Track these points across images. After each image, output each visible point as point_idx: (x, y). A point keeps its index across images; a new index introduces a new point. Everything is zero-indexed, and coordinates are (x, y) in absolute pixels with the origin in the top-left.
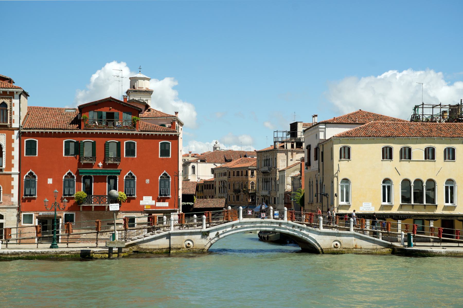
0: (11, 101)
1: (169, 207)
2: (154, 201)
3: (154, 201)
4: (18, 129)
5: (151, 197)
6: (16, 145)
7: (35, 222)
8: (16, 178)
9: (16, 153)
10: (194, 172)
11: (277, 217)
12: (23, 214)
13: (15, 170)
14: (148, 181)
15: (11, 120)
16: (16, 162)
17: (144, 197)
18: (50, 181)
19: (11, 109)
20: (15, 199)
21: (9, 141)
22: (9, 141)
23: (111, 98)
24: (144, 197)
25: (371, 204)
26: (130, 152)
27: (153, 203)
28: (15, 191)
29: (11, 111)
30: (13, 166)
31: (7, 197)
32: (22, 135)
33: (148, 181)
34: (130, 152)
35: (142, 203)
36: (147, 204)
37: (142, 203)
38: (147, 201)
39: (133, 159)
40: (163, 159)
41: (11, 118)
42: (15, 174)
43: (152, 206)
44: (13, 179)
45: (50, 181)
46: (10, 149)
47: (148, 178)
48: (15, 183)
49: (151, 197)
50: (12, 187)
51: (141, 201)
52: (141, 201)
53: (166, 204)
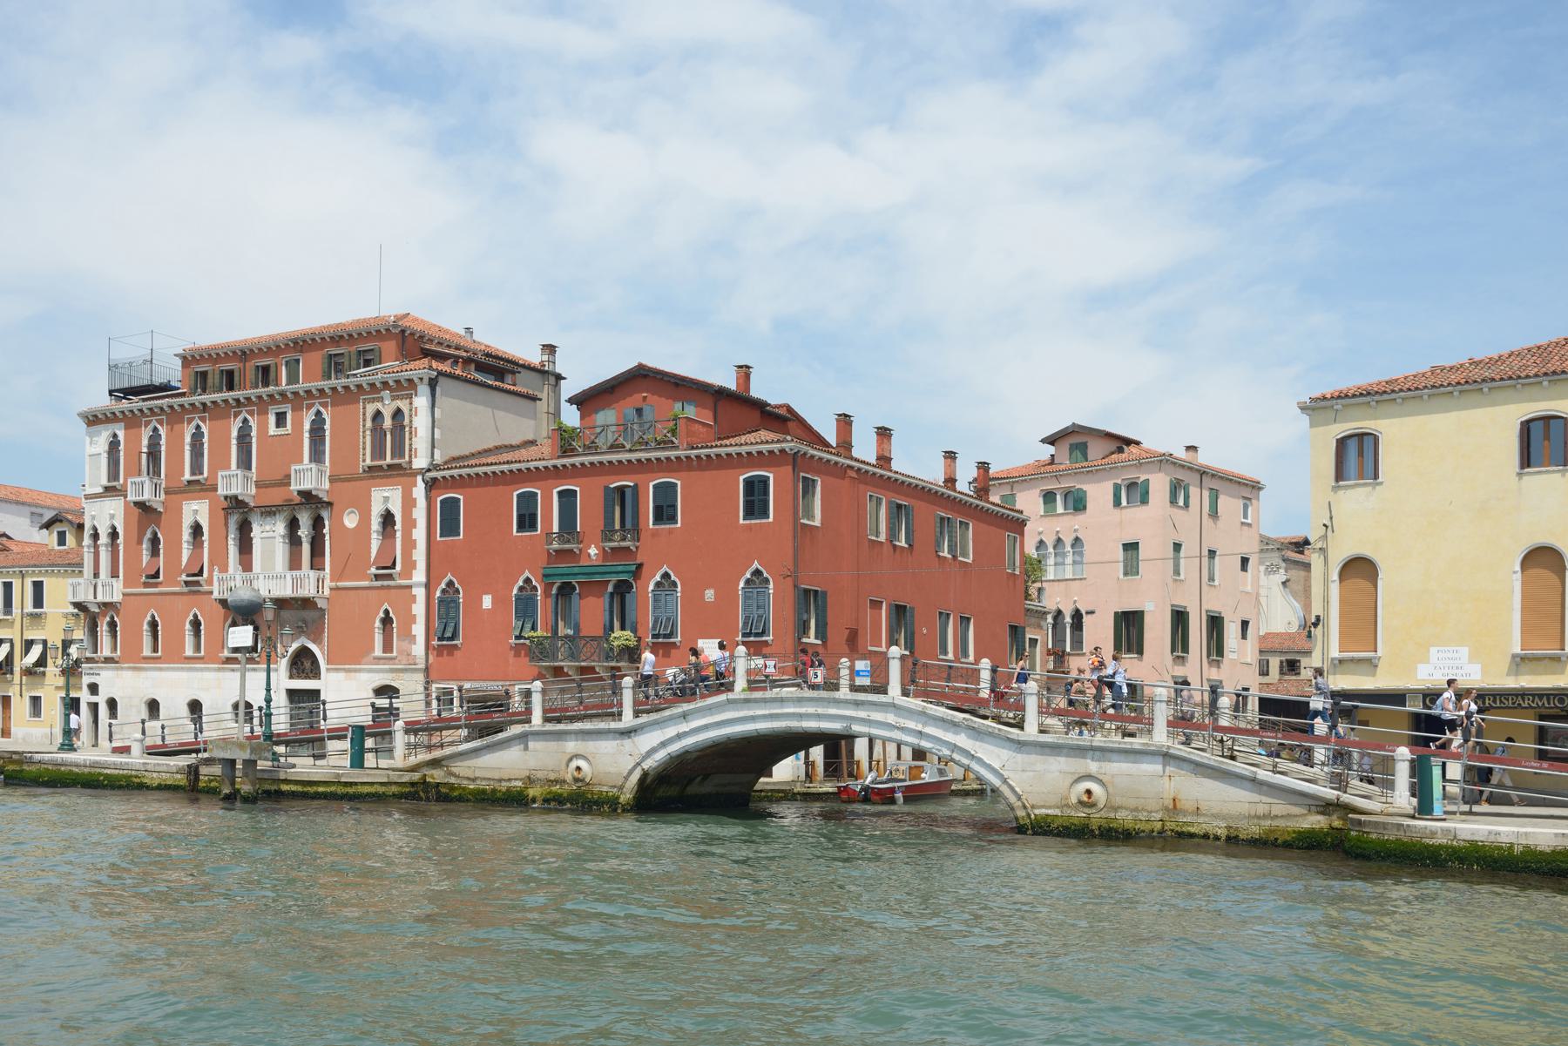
4: (423, 472)
6: (420, 513)
8: (420, 593)
9: (419, 534)
11: (866, 681)
12: (434, 686)
13: (419, 576)
14: (710, 595)
18: (487, 602)
20: (419, 649)
21: (409, 503)
22: (409, 503)
23: (641, 367)
26: (665, 513)
28: (419, 629)
30: (413, 565)
31: (405, 644)
32: (431, 485)
33: (710, 595)
34: (665, 513)
39: (671, 531)
40: (749, 527)
42: (418, 585)
44: (413, 599)
45: (487, 602)
46: (410, 523)
47: (709, 587)
48: (419, 609)
50: (413, 619)
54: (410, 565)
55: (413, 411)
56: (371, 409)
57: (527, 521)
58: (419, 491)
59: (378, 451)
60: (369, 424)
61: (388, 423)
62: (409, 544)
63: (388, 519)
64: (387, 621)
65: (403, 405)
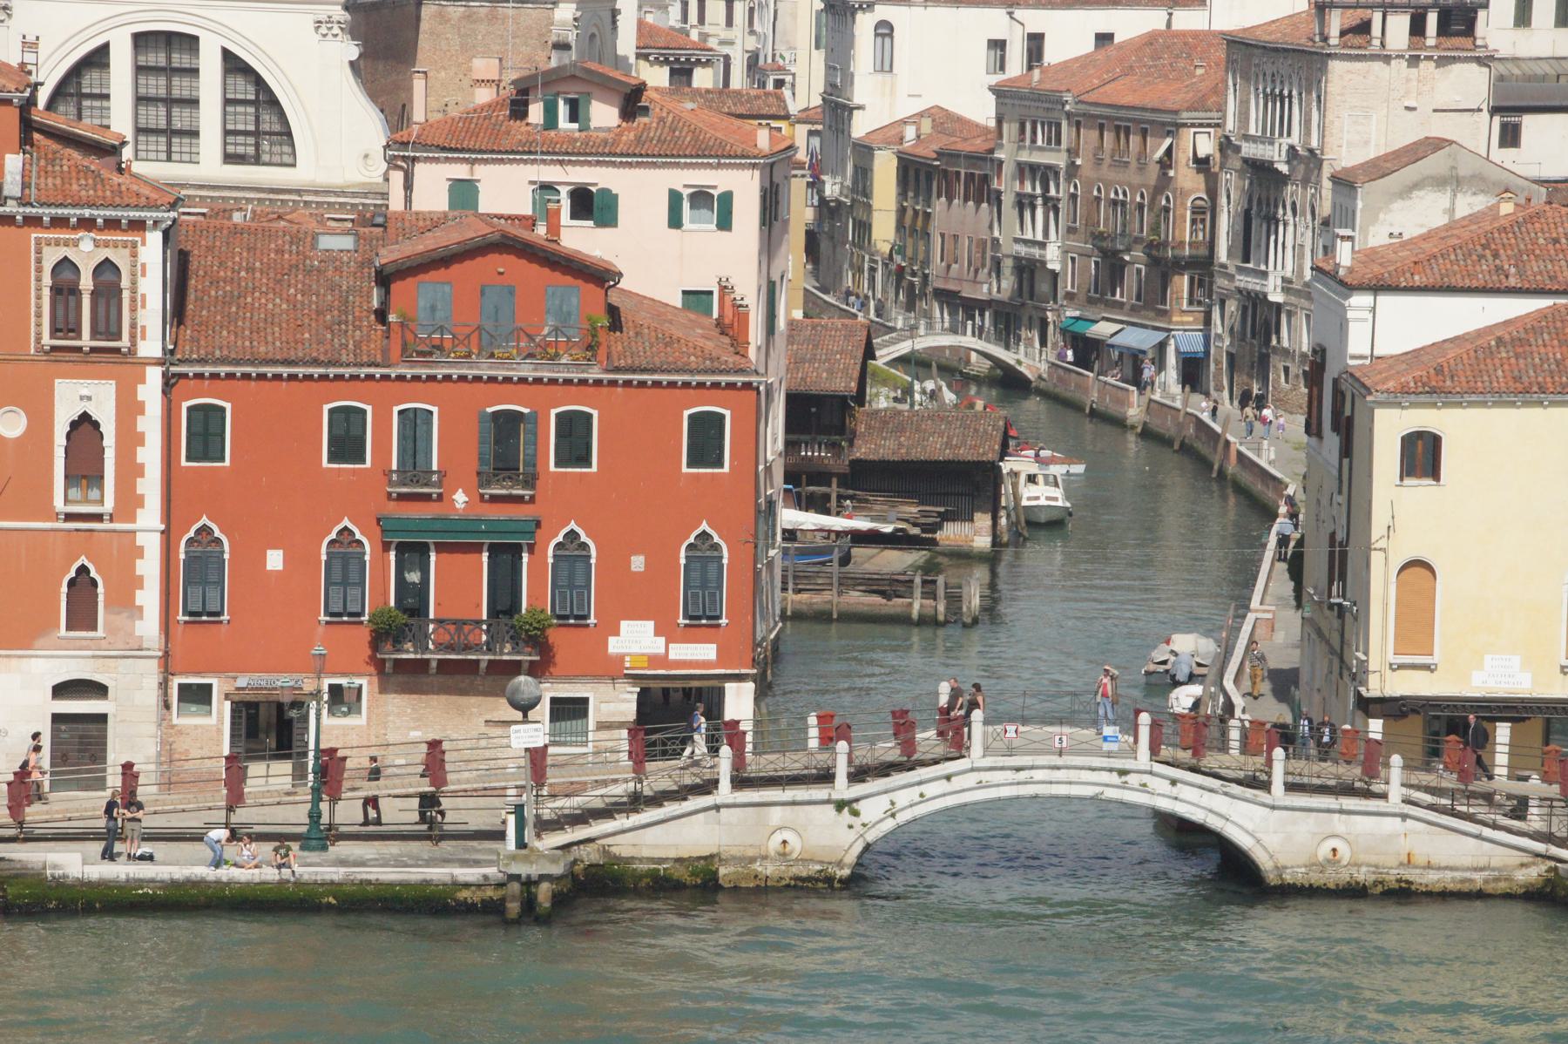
0: (134, 255)
1: (722, 659)
2: (662, 640)
3: (662, 640)
5: (650, 625)
6: (151, 424)
7: (221, 714)
8: (151, 544)
9: (150, 455)
10: (885, 65)
12: (176, 681)
14: (638, 563)
15: (133, 326)
16: (150, 486)
17: (624, 624)
18: (275, 560)
19: (134, 283)
20: (149, 626)
21: (129, 408)
22: (129, 408)
24: (624, 624)
25: (1516, 660)
27: (657, 645)
28: (149, 598)
29: (134, 291)
30: (139, 501)
32: (169, 382)
33: (638, 563)
35: (615, 646)
36: (635, 649)
37: (615, 646)
38: (636, 640)
41: (133, 326)
43: (654, 660)
44: (139, 552)
45: (275, 560)
46: (130, 439)
48: (149, 567)
49: (650, 625)
50: (138, 582)
51: (612, 640)
52: (612, 640)
53: (706, 652)
54: (129, 503)
55: (138, 271)
56: (51, 257)
57: (347, 445)
58: (151, 389)
59: (65, 325)
60: (47, 280)
61: (86, 283)
62: (130, 470)
63: (84, 425)
64: (82, 584)
65: (120, 258)
